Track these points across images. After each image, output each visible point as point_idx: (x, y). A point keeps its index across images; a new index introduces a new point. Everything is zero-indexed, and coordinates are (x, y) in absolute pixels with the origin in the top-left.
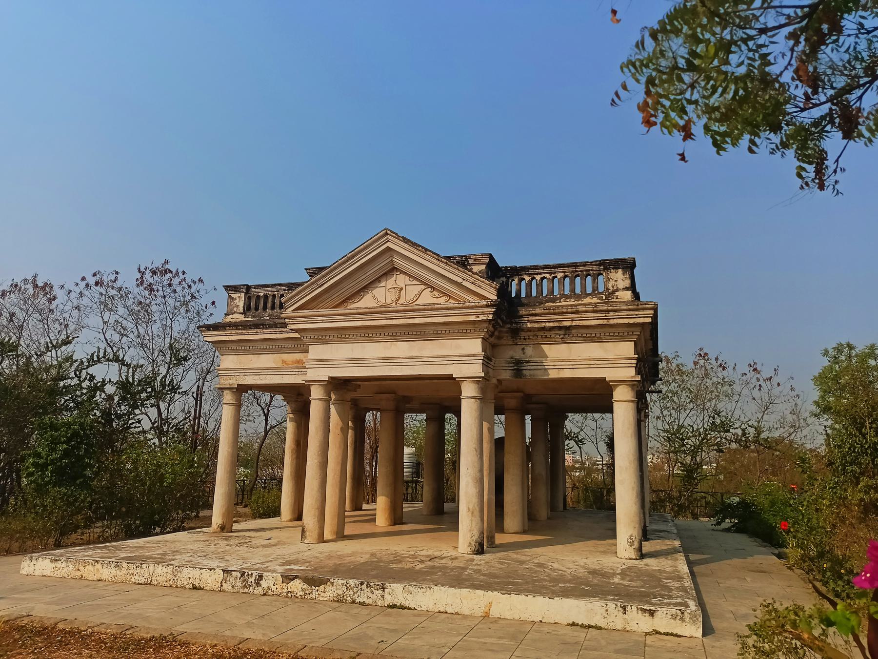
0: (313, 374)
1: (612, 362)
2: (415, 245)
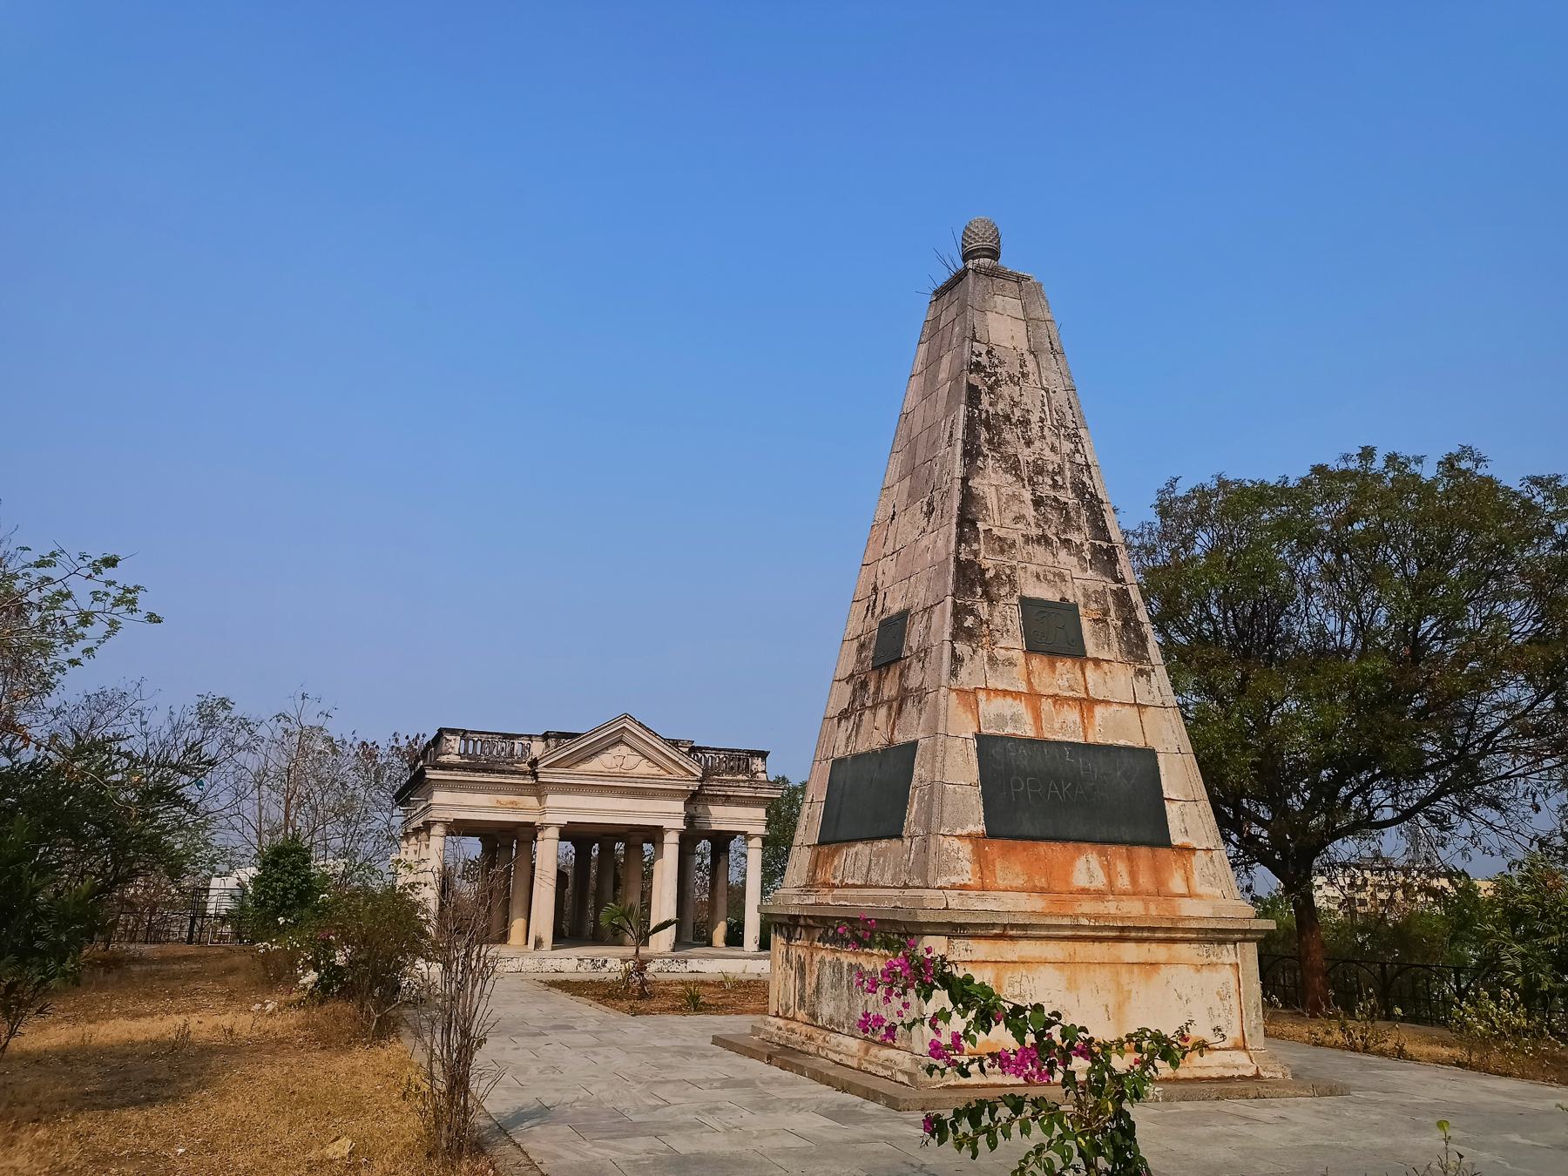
0: (548, 819)
1: (752, 822)
2: (648, 729)
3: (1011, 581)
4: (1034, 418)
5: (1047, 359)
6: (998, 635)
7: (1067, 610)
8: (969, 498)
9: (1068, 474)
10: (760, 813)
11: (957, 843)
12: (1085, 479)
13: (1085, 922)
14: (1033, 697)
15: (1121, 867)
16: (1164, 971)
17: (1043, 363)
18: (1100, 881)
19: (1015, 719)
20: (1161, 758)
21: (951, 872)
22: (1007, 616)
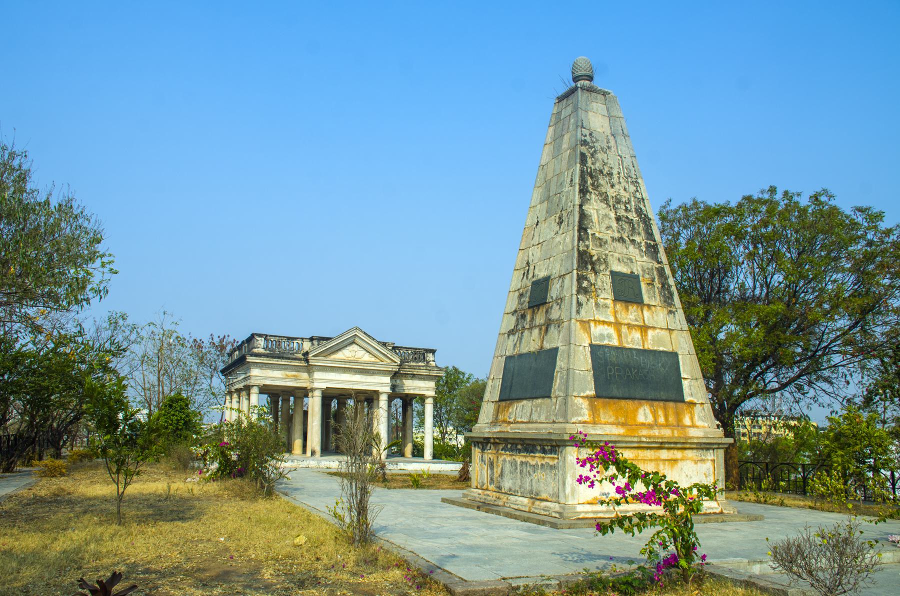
0: (316, 385)
1: (428, 389)
2: (369, 336)
3: (606, 262)
4: (615, 172)
5: (620, 139)
6: (599, 291)
7: (633, 278)
8: (583, 216)
9: (633, 203)
10: (432, 384)
11: (581, 400)
12: (642, 206)
13: (644, 439)
14: (617, 325)
15: (661, 413)
16: (680, 464)
17: (619, 141)
18: (650, 419)
19: (609, 337)
20: (680, 357)
21: (579, 415)
22: (604, 281)
